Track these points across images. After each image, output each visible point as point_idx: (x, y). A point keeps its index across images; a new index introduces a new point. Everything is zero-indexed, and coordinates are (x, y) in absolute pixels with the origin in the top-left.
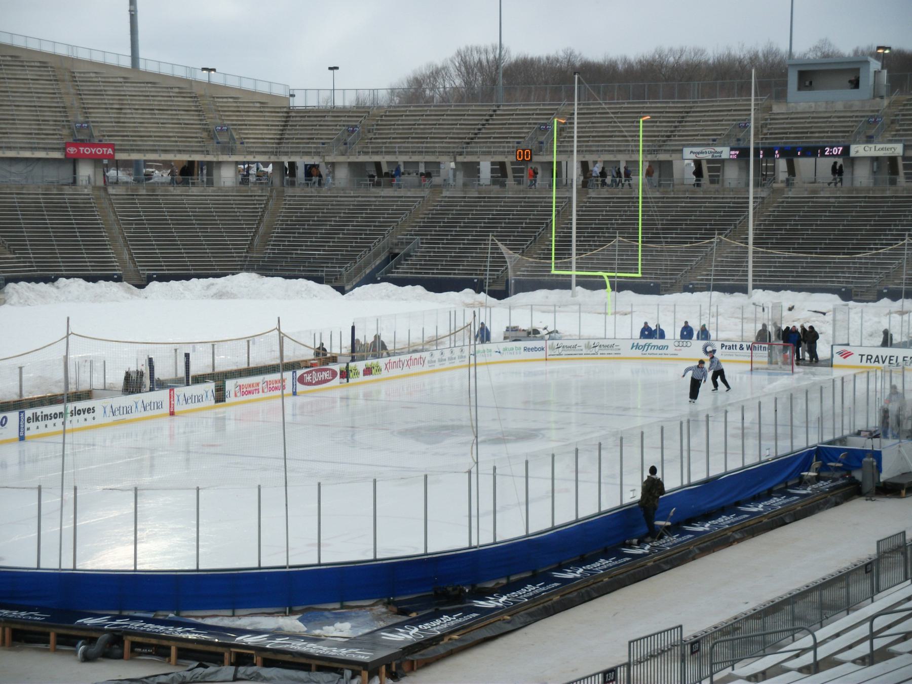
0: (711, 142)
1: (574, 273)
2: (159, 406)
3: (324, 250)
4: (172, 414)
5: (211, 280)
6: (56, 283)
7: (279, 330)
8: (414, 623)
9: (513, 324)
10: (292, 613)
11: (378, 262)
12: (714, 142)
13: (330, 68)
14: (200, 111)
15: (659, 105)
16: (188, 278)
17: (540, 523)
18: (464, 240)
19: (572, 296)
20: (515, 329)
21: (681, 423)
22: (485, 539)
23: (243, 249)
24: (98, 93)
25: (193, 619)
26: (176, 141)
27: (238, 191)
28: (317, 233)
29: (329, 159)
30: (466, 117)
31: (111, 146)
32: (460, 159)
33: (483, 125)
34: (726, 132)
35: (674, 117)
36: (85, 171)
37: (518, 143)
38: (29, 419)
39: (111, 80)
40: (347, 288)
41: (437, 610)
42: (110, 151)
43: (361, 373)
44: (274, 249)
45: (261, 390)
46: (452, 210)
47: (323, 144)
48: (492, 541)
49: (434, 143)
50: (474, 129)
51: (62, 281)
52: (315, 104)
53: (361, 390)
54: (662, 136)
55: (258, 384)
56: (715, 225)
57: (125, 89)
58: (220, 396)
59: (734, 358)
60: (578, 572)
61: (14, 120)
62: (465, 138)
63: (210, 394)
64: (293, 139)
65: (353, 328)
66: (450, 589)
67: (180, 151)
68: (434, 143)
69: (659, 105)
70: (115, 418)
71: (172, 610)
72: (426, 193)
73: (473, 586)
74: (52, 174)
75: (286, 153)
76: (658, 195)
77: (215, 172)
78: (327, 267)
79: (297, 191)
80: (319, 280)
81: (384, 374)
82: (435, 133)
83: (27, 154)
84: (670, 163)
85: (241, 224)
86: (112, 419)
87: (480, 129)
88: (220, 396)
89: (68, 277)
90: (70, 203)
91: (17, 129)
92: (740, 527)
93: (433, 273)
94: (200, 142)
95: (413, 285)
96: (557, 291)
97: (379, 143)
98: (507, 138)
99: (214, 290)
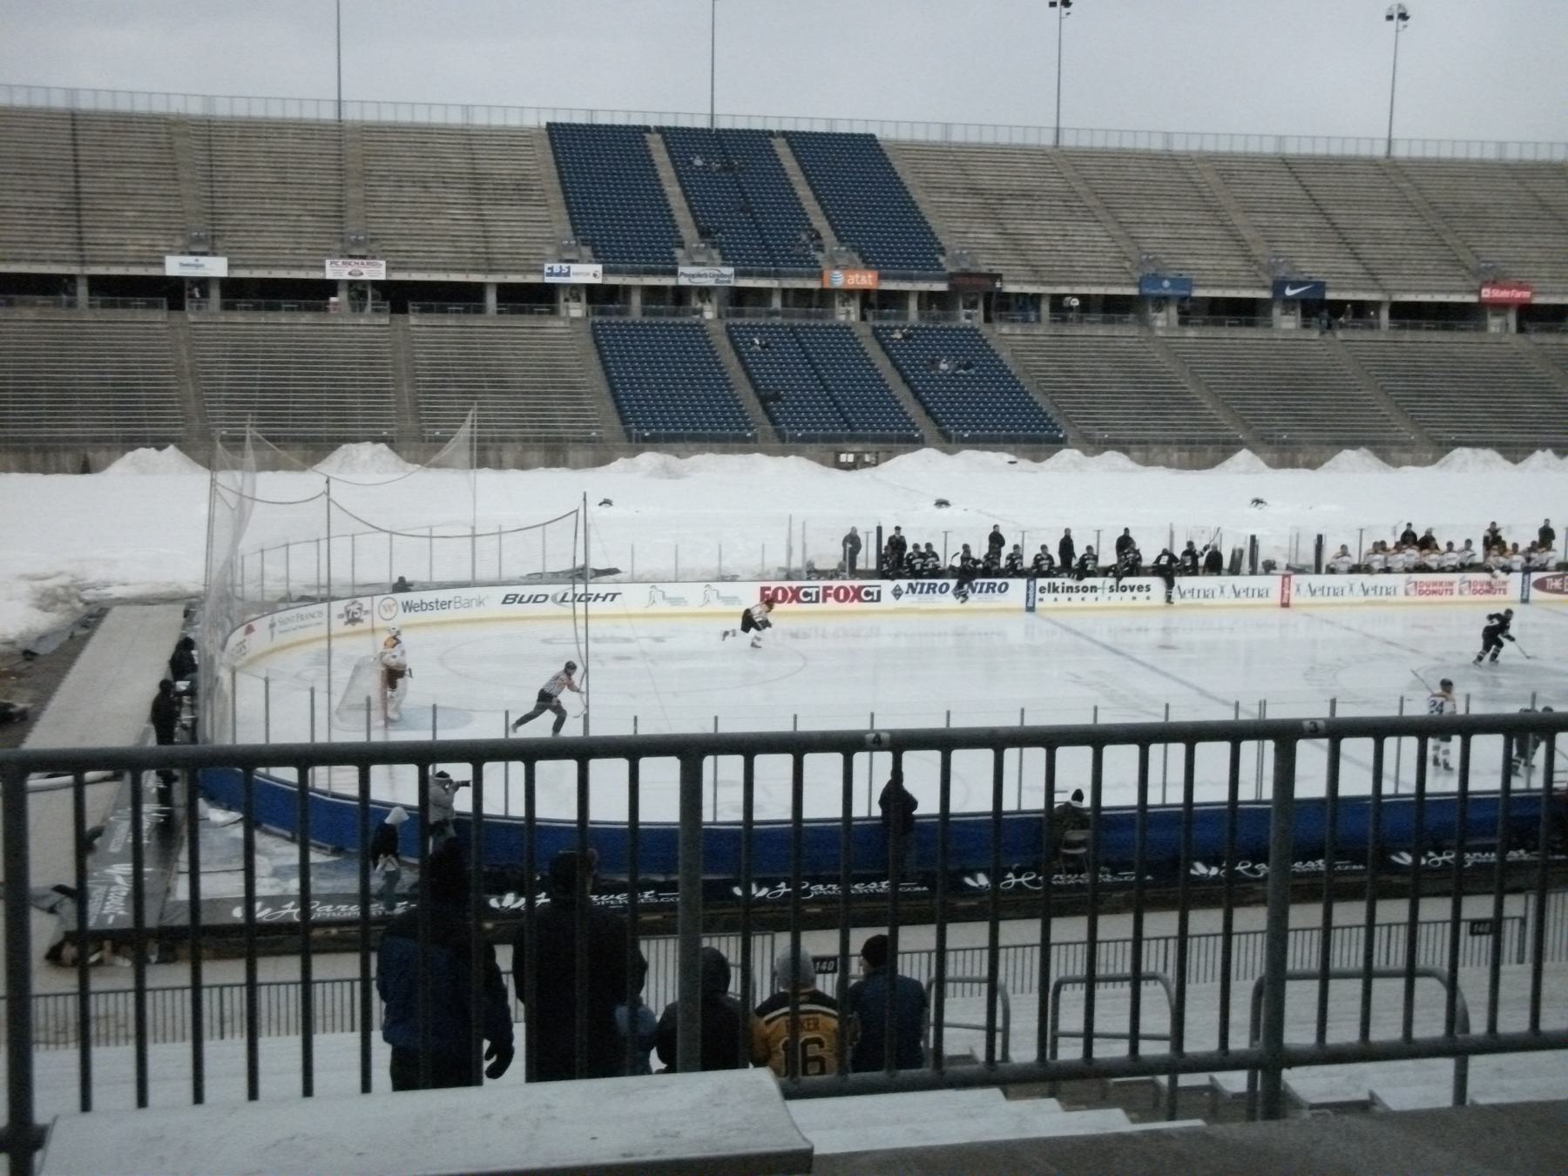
4: (1285, 605)
38: (1042, 590)
45: (1456, 591)
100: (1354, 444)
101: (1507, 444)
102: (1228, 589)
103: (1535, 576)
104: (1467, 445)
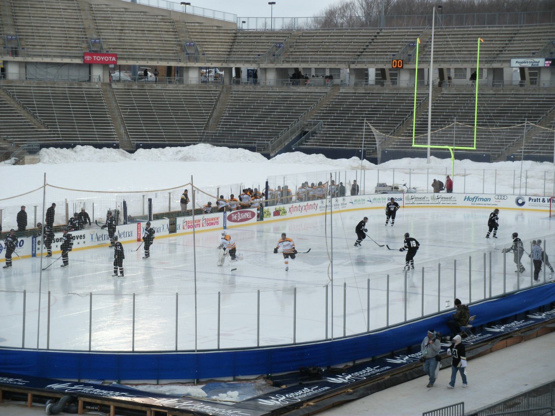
0: (531, 55)
1: (429, 146)
2: (130, 234)
3: (257, 129)
5: (179, 148)
6: (74, 149)
7: (192, 184)
8: (282, 392)
9: (381, 182)
10: (199, 383)
11: (293, 138)
12: (534, 55)
13: (270, 3)
14: (176, 32)
15: (495, 29)
16: (163, 146)
17: (378, 323)
18: (353, 122)
19: (427, 163)
20: (384, 185)
21: (485, 254)
22: (338, 334)
23: (202, 127)
24: (106, 19)
25: (129, 386)
26: (159, 53)
27: (200, 87)
28: (252, 117)
29: (263, 66)
30: (358, 37)
31: (115, 55)
32: (353, 66)
33: (370, 43)
34: (542, 48)
35: (506, 37)
36: (97, 72)
37: (394, 55)
39: (116, 10)
40: (271, 155)
41: (300, 384)
42: (114, 59)
43: (272, 214)
44: (223, 128)
45: (201, 225)
46: (346, 102)
47: (259, 55)
48: (342, 335)
49: (335, 55)
50: (363, 45)
51: (79, 147)
52: (255, 28)
53: (272, 226)
54: (496, 51)
55: (199, 221)
56: (532, 113)
57: (125, 16)
58: (173, 229)
59: (538, 208)
60: (405, 359)
61: (50, 37)
62: (357, 52)
63: (166, 227)
64: (238, 52)
65: (267, 183)
66: (311, 369)
67: (161, 60)
68: (335, 55)
69: (495, 29)
70: (99, 242)
71: (114, 379)
72: (328, 90)
73: (329, 367)
74: (75, 74)
75: (233, 62)
76: (491, 92)
77: (185, 74)
78: (259, 140)
79: (240, 88)
80: (253, 149)
81: (288, 215)
82: (336, 48)
83: (58, 60)
84: (501, 70)
85: (201, 110)
86: (96, 243)
87: (367, 46)
88: (173, 229)
90: (86, 94)
91: (52, 43)
92: (526, 329)
93: (331, 146)
94: (175, 53)
95: (317, 153)
96: (417, 159)
97: (297, 55)
98: (386, 52)
99: (180, 155)
103: (228, 213)
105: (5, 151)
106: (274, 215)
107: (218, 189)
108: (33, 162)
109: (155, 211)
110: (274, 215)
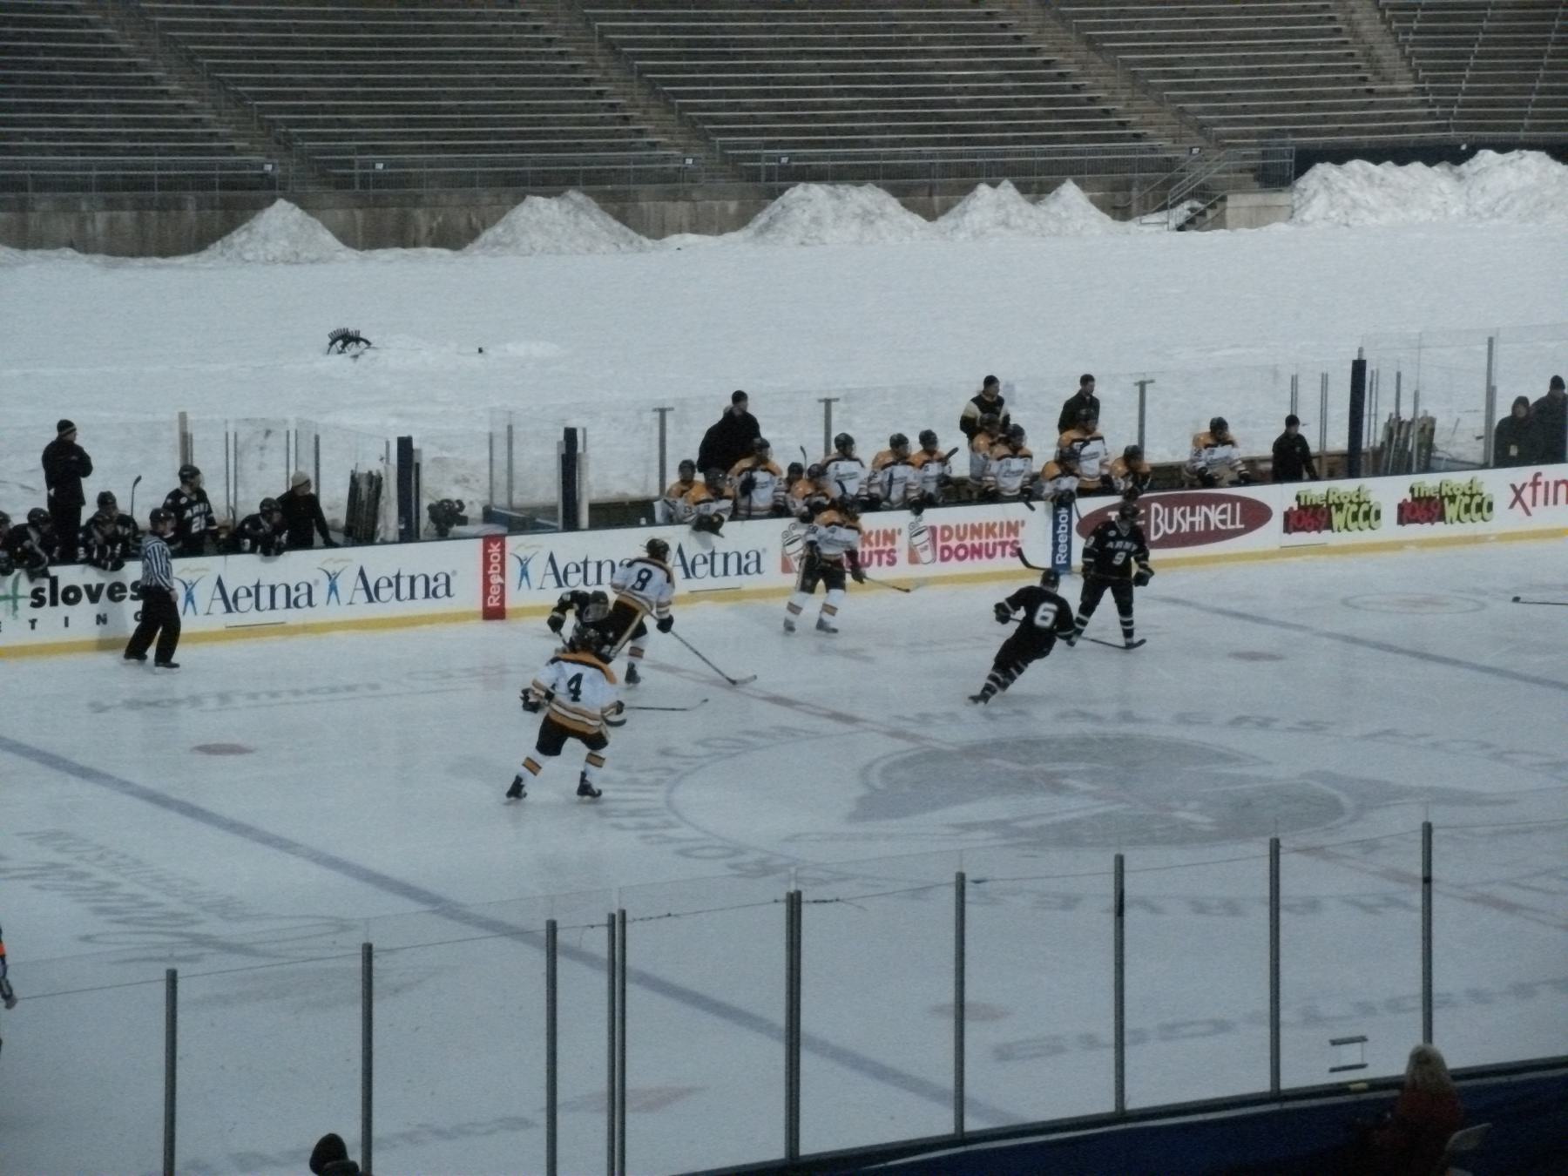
4: (494, 613)
6: (1464, 166)
43: (1390, 514)
51: (1487, 157)
65: (1359, 368)
70: (235, 619)
81: (1504, 519)
89: (1503, 147)
100: (551, 184)
101: (905, 172)
102: (348, 583)
104: (818, 176)
105: (1165, 176)
106: (1401, 521)
107: (1142, 385)
108: (1256, 220)
109: (598, 483)
110: (1401, 521)
